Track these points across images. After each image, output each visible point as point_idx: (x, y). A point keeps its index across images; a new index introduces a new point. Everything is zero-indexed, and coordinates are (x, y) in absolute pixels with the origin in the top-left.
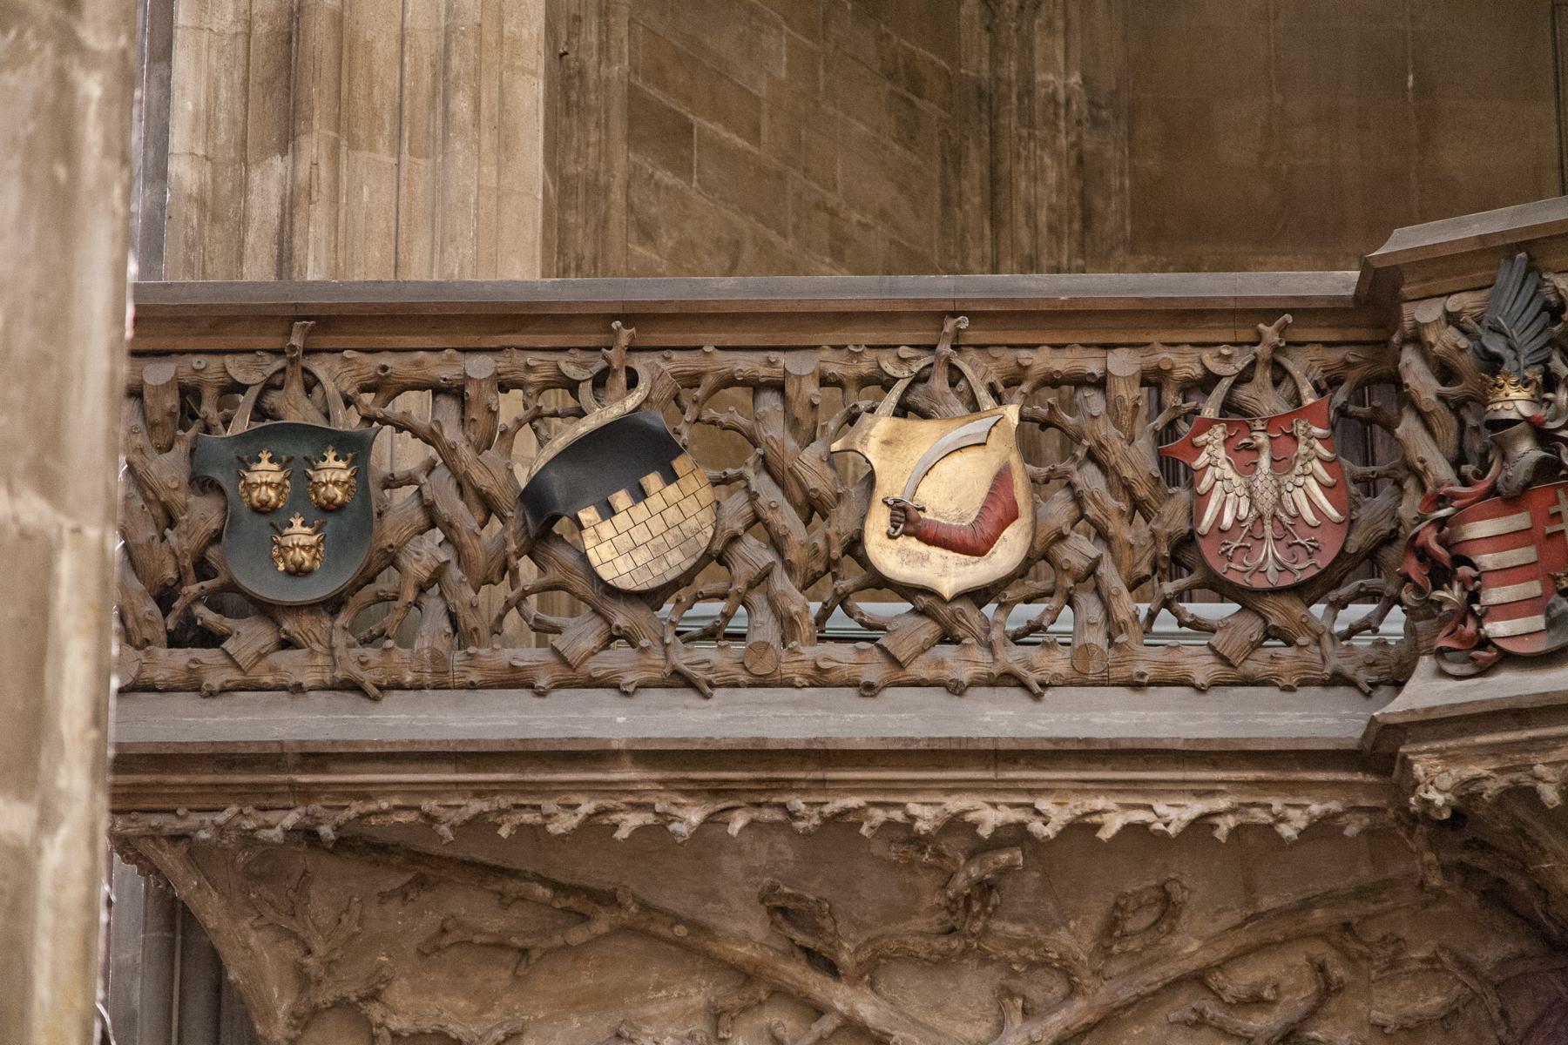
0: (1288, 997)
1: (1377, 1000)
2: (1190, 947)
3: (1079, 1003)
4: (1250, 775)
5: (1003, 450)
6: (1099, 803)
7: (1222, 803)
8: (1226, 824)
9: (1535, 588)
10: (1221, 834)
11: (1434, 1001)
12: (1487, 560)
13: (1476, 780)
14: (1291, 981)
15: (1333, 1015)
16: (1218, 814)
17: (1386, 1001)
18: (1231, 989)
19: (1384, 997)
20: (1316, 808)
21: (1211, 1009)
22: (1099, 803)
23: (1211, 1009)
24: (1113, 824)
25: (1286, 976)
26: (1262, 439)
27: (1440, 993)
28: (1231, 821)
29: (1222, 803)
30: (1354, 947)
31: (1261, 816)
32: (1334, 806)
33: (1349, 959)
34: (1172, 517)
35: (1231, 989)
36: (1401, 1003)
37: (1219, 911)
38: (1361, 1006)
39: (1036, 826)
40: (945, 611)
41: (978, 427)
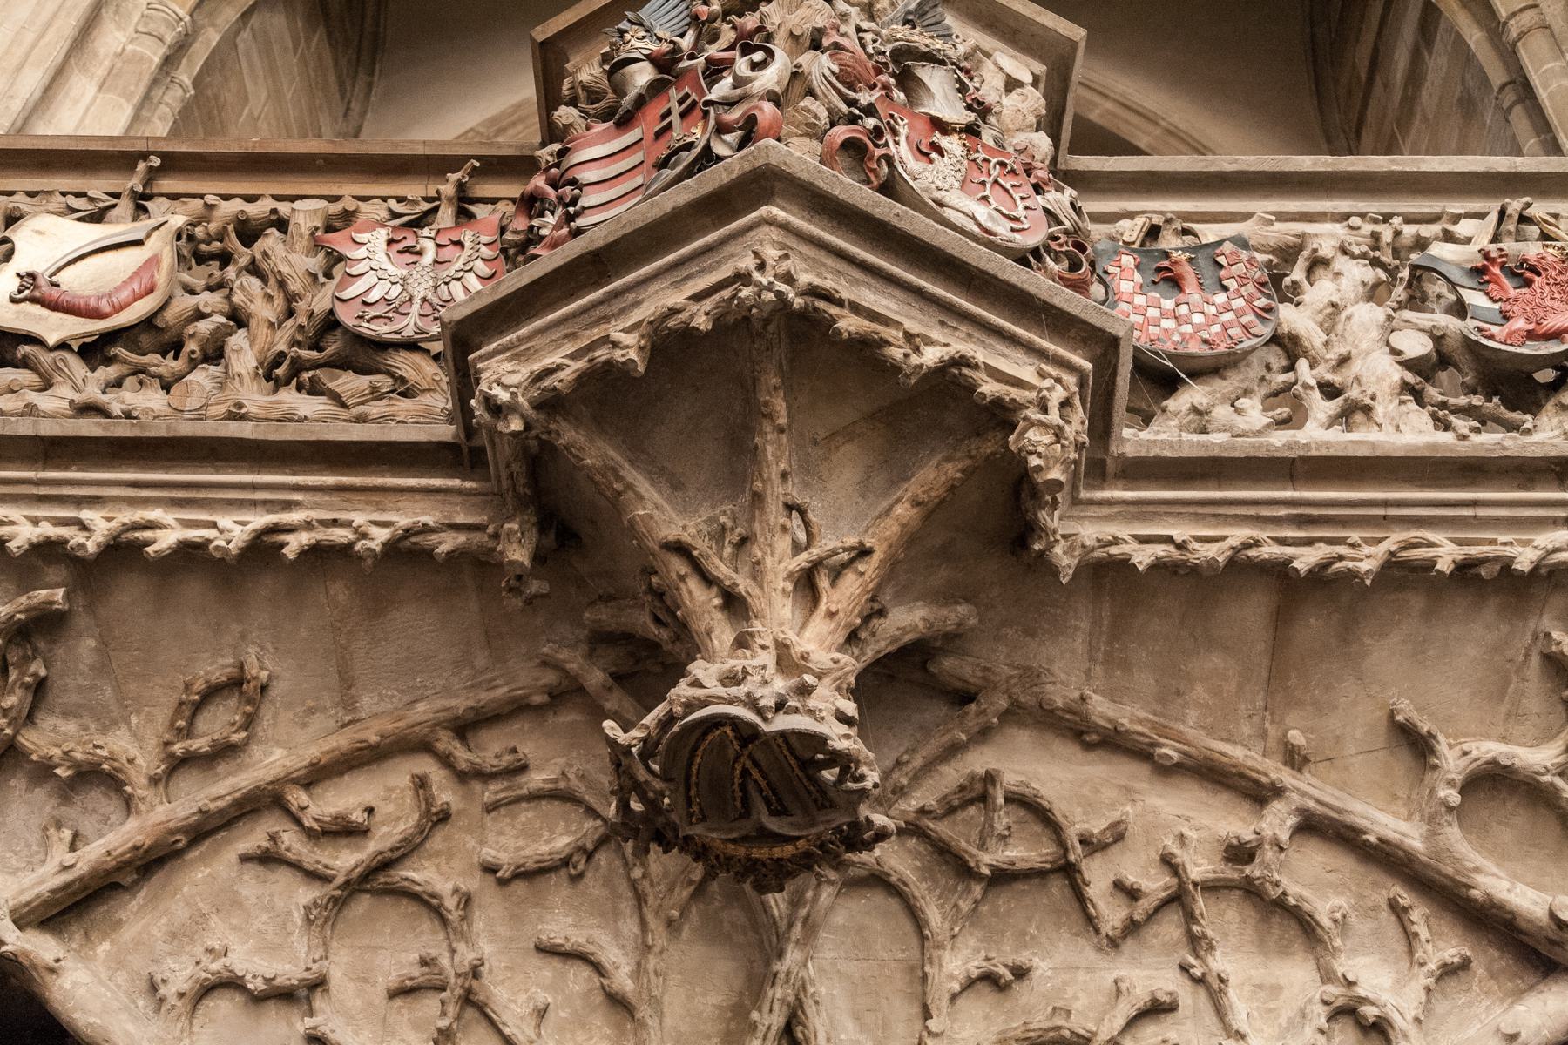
0: (385, 829)
1: (491, 837)
2: (270, 760)
3: (132, 823)
4: (330, 480)
5: (161, 246)
6: (155, 514)
7: (295, 517)
8: (294, 544)
9: (639, 180)
10: (290, 552)
11: (562, 842)
12: (588, 175)
13: (549, 372)
14: (390, 808)
15: (437, 854)
16: (291, 529)
17: (502, 839)
18: (314, 810)
19: (501, 833)
20: (403, 521)
21: (291, 841)
22: (155, 514)
23: (291, 841)
24: (165, 540)
25: (384, 799)
26: (429, 246)
27: (568, 832)
28: (304, 539)
29: (295, 517)
30: (462, 756)
31: (340, 535)
32: (429, 519)
33: (464, 777)
34: (320, 302)
35: (314, 810)
36: (521, 843)
37: (311, 711)
38: (471, 843)
39: (75, 537)
40: (45, 358)
41: (136, 230)
